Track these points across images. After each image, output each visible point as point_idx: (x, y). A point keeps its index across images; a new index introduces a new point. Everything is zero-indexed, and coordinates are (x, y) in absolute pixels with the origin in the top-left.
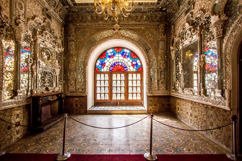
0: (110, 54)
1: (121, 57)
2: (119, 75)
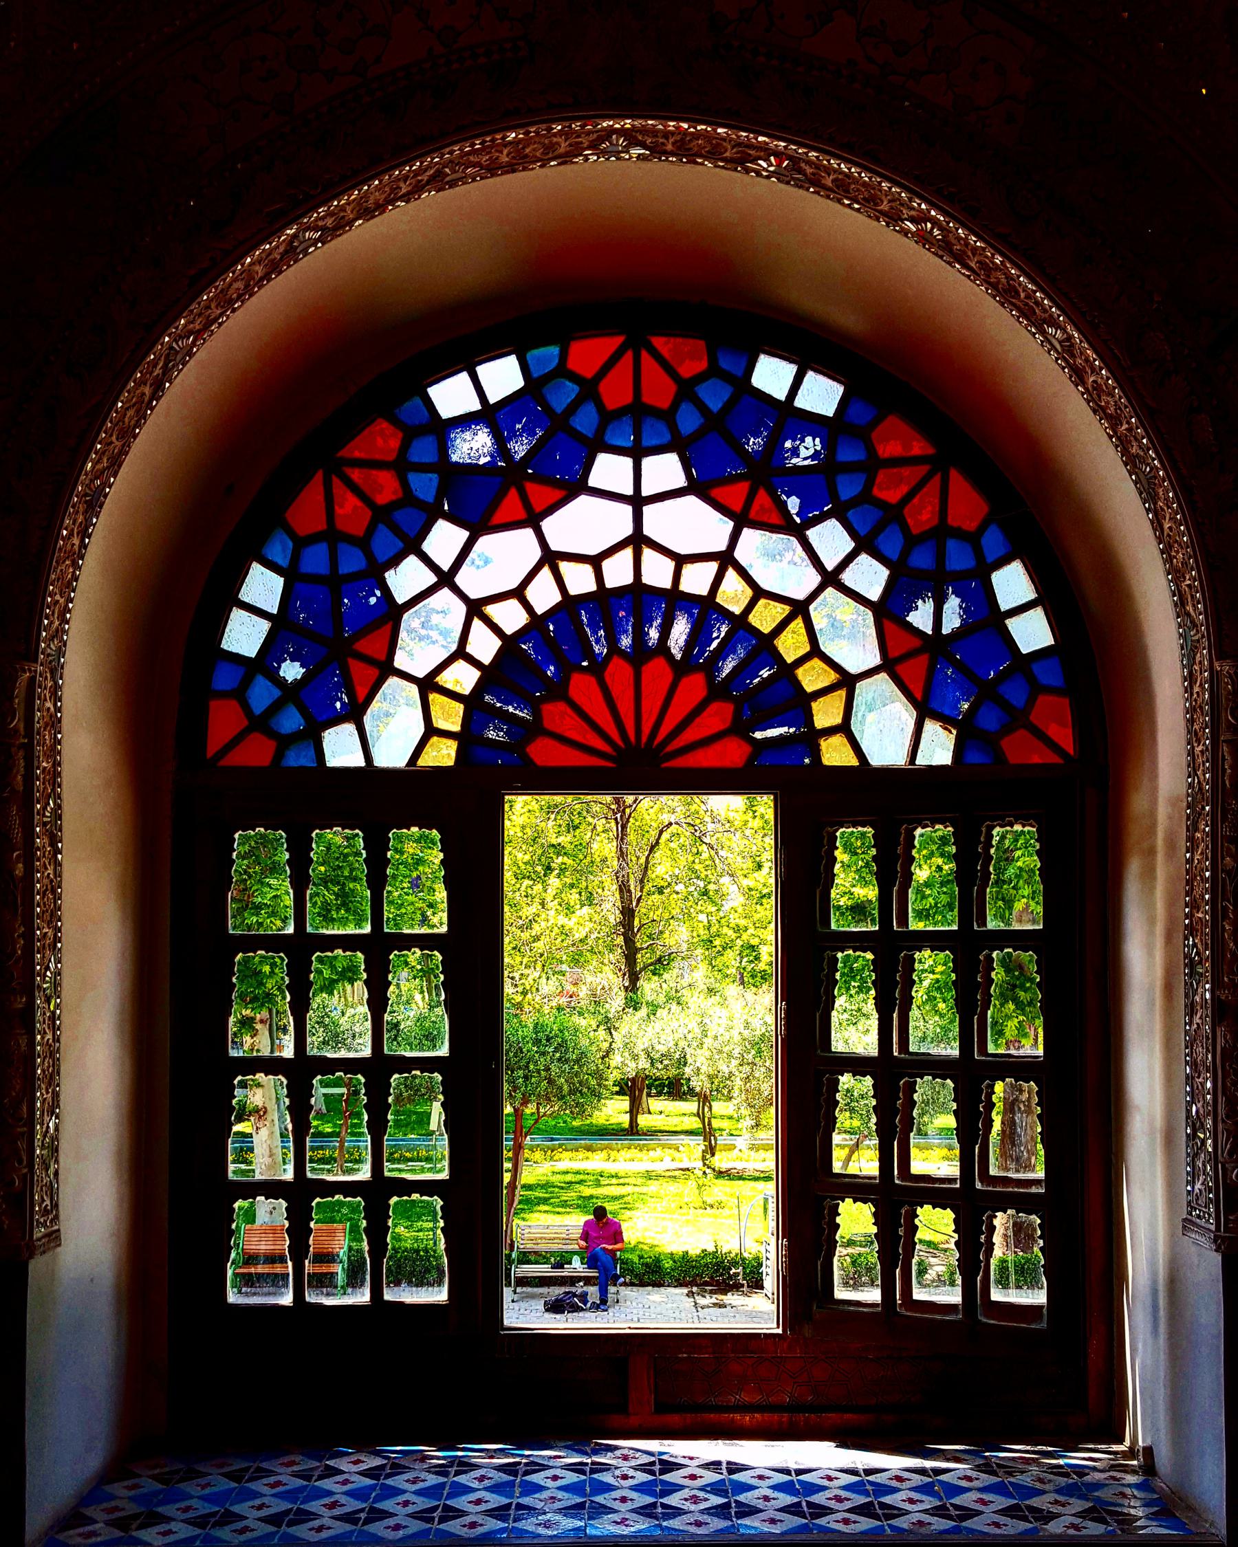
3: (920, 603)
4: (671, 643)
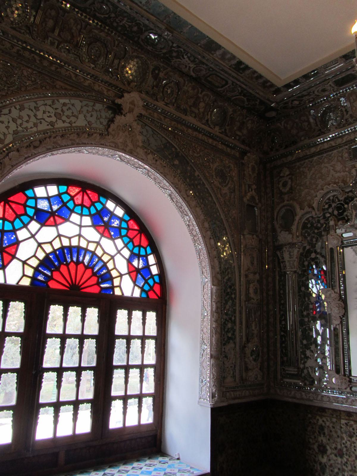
0: (43, 205)
1: (92, 229)
2: (75, 311)
3: (135, 260)
4: (85, 261)
